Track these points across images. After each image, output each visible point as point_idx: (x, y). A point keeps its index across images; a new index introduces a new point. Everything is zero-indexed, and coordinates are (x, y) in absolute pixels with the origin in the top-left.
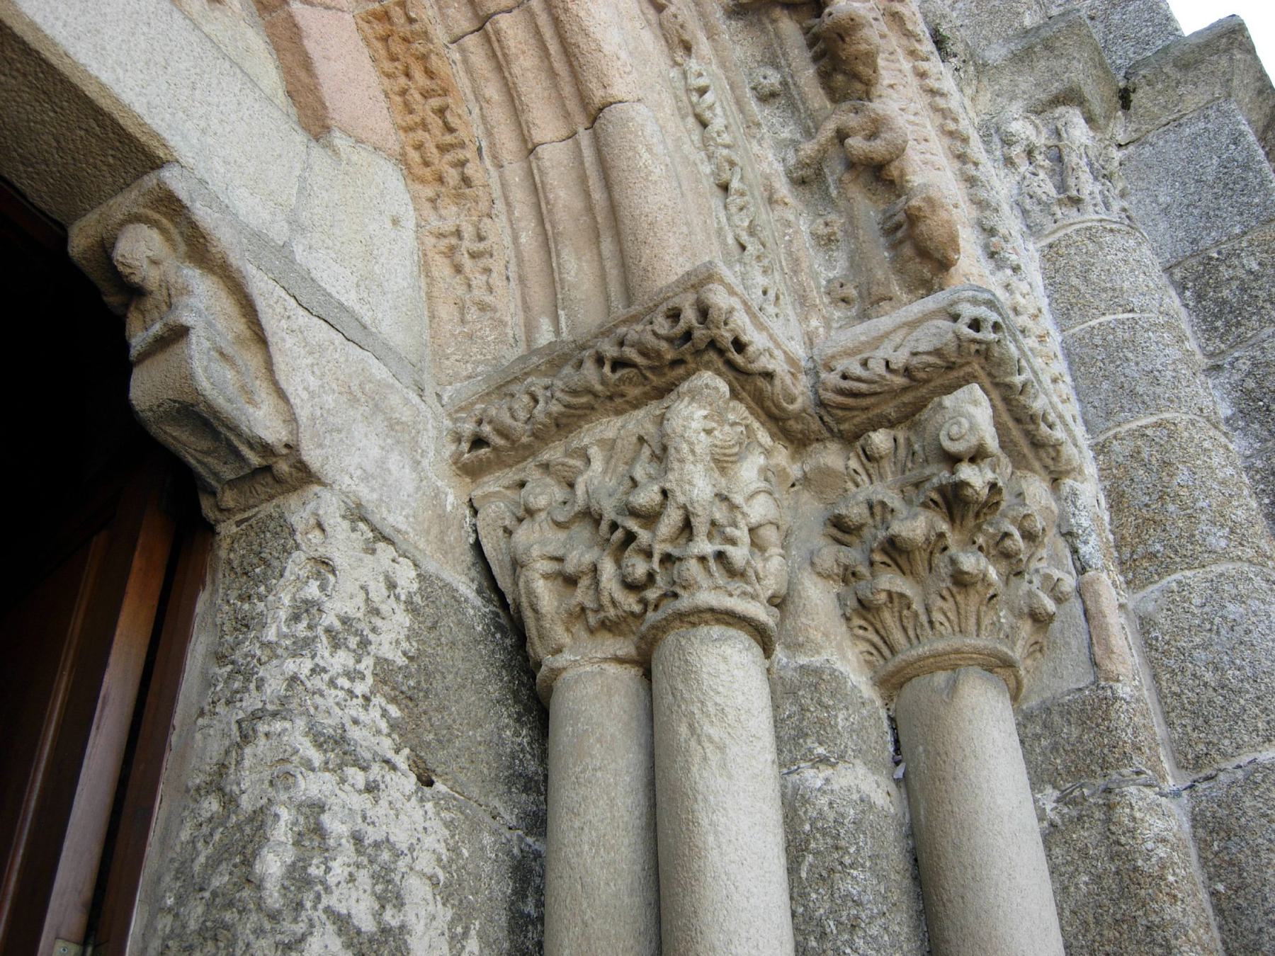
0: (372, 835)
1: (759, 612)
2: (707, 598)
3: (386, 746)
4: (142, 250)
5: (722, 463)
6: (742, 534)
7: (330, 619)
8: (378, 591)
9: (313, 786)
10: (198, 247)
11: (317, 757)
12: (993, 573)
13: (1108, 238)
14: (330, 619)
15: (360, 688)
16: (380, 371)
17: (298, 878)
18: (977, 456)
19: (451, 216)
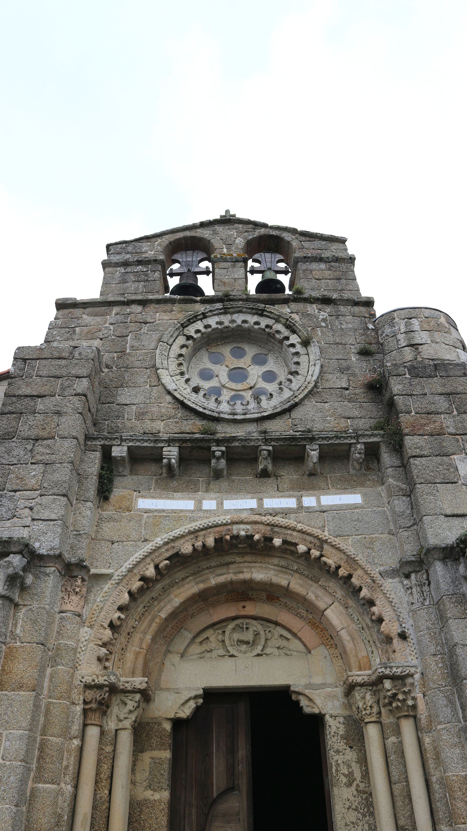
0: (345, 760)
1: (374, 719)
2: (367, 720)
3: (344, 747)
4: (294, 697)
5: (364, 698)
6: (368, 708)
7: (332, 734)
8: (338, 725)
9: (336, 758)
10: (299, 693)
11: (335, 754)
12: (399, 704)
13: (418, 612)
14: (332, 734)
15: (339, 741)
16: (329, 690)
17: (337, 771)
18: (389, 690)
19: (332, 651)
